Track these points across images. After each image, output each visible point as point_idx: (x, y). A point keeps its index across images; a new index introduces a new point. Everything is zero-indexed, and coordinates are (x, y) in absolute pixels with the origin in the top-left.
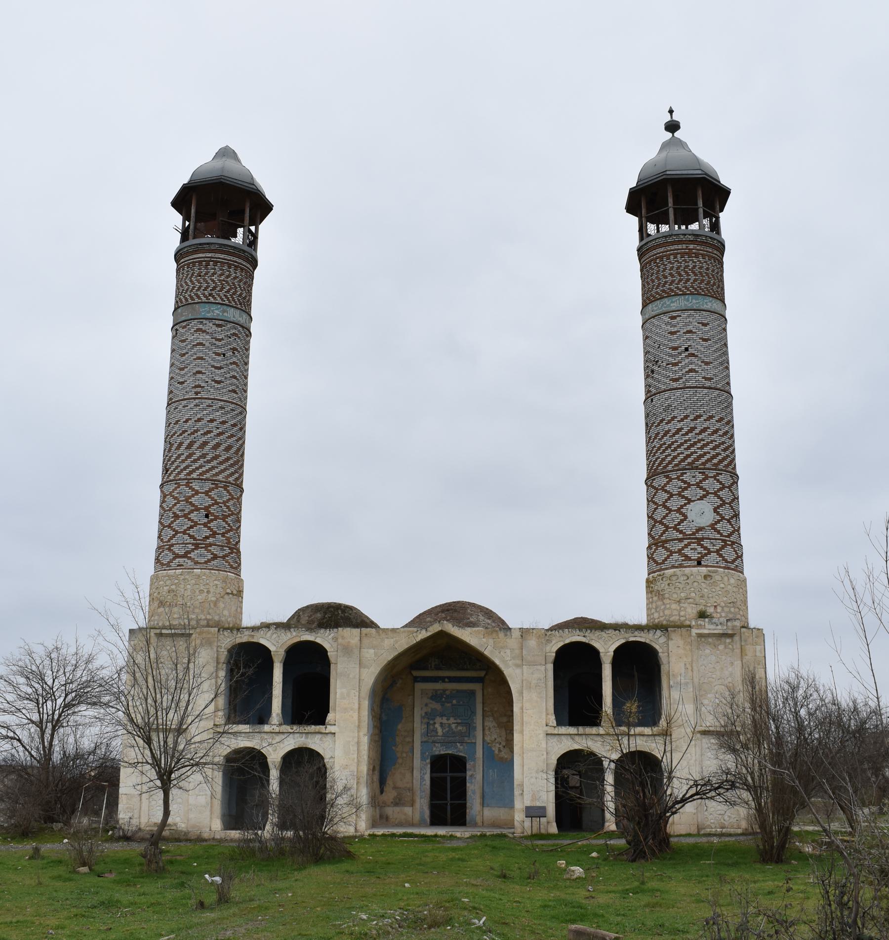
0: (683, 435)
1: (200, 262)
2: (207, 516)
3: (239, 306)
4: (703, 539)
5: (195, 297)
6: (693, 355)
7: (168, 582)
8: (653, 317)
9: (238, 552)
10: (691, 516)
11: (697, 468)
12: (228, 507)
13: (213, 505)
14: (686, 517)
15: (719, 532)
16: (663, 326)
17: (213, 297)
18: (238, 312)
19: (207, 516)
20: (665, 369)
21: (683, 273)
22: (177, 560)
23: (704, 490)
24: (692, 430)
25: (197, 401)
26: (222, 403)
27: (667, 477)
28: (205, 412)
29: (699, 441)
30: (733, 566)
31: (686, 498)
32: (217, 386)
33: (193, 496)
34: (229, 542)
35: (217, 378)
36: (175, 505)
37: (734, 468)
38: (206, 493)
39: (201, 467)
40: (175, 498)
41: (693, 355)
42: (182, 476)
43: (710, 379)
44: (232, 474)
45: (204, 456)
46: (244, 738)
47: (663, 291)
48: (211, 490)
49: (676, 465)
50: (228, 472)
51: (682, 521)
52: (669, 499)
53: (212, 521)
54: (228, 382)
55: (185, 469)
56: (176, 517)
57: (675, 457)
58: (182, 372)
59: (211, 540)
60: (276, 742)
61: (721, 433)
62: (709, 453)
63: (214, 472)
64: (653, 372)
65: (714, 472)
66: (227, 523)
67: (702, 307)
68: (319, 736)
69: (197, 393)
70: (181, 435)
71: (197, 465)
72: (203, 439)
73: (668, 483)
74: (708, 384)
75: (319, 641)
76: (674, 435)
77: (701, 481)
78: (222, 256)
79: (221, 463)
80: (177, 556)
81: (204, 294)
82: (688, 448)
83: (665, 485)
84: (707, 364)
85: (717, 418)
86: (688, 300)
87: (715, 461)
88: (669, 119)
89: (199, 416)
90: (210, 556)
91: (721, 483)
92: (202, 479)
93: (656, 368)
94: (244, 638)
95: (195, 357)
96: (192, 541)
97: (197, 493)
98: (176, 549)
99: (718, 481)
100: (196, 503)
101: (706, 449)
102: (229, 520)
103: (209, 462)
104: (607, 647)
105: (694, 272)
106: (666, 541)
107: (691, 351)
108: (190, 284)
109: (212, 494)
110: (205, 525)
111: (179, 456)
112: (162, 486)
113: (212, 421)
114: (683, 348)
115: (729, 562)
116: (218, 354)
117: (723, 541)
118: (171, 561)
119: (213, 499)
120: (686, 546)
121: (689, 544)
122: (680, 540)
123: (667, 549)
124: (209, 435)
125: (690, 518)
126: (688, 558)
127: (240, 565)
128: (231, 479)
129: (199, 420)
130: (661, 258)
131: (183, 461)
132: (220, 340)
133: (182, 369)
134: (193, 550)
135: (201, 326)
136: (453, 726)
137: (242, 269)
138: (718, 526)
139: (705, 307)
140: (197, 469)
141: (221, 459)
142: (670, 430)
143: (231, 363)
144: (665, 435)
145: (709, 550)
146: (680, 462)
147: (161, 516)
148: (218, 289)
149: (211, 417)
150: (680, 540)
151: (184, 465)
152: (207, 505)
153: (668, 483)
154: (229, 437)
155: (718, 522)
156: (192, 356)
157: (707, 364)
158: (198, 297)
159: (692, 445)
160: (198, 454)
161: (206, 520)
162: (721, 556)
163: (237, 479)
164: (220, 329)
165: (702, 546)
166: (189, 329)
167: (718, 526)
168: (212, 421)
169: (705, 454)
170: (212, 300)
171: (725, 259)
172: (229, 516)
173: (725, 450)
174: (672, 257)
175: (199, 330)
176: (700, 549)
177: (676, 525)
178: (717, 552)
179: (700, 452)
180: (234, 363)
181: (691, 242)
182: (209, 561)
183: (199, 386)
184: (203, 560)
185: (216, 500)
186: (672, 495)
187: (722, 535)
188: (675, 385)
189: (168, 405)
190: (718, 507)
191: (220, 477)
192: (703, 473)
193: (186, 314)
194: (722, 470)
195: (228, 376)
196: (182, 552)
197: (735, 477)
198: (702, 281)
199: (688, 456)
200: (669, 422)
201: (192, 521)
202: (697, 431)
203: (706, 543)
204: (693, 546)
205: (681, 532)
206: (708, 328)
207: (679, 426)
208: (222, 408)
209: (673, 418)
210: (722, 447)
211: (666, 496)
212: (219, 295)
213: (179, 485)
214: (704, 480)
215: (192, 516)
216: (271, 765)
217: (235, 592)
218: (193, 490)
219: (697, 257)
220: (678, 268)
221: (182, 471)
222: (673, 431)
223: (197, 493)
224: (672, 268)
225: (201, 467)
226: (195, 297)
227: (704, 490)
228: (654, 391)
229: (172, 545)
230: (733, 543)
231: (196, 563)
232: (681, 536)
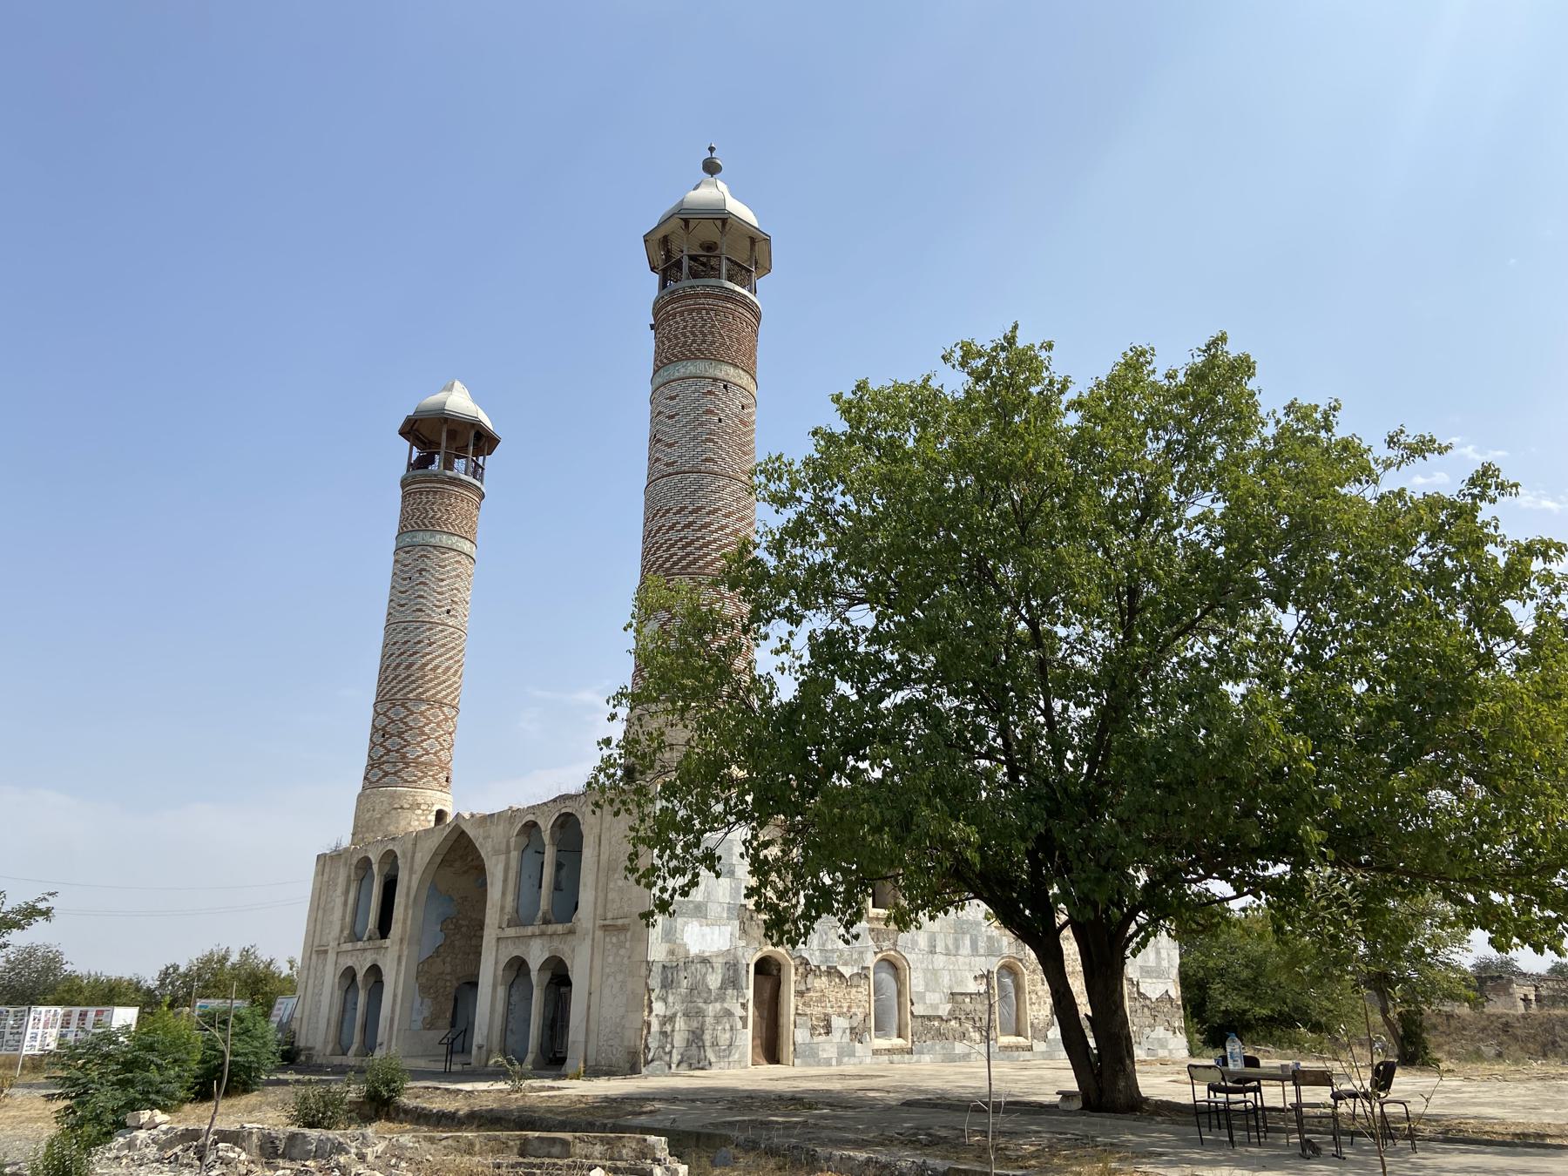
6: (659, 441)
34: (404, 756)
38: (385, 714)
41: (659, 441)
84: (670, 446)
87: (668, 565)
102: (406, 736)
104: (546, 825)
157: (670, 446)
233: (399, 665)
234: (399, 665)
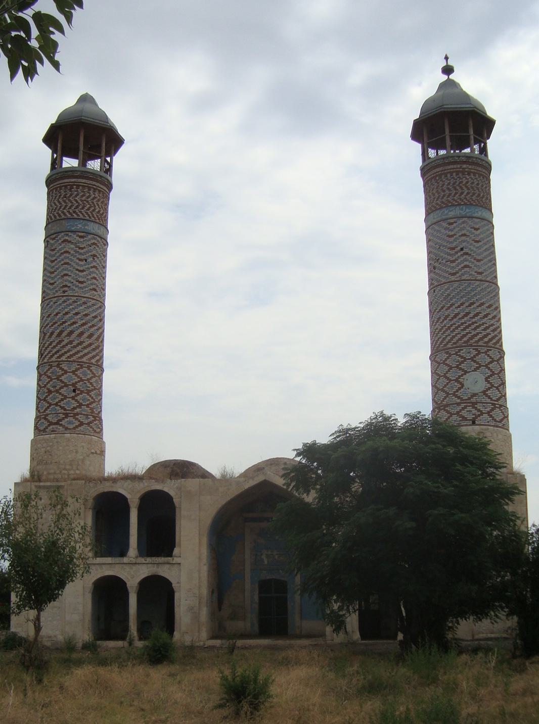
0: (459, 319)
1: (66, 186)
2: (74, 391)
3: (98, 221)
4: (476, 403)
5: (62, 214)
6: (467, 254)
7: (45, 445)
8: (435, 224)
9: (101, 420)
10: (467, 384)
11: (471, 345)
12: (91, 383)
13: (79, 382)
14: (463, 385)
15: (489, 397)
16: (443, 231)
17: (77, 214)
18: (97, 225)
19: (74, 391)
20: (445, 265)
21: (458, 188)
22: (51, 427)
23: (477, 363)
24: (467, 314)
25: (65, 298)
26: (85, 299)
27: (447, 353)
28: (71, 307)
29: (473, 323)
30: (500, 425)
31: (463, 370)
32: (80, 285)
33: (63, 375)
34: (93, 412)
35: (81, 279)
36: (48, 382)
37: (501, 345)
38: (73, 372)
39: (69, 351)
40: (49, 377)
41: (467, 254)
42: (54, 359)
43: (480, 273)
44: (94, 357)
45: (71, 342)
46: (106, 567)
47: (443, 202)
48: (77, 370)
49: (455, 343)
50: (90, 355)
51: (460, 389)
52: (449, 371)
53: (78, 394)
54: (89, 282)
55: (56, 353)
56: (50, 392)
57: (454, 337)
58: (53, 275)
59: (78, 410)
60: (133, 570)
61: (490, 317)
62: (481, 333)
63: (79, 355)
64: (435, 268)
65: (486, 349)
66: (90, 396)
67: (474, 215)
68: (168, 566)
69: (64, 292)
70: (52, 325)
71: (65, 350)
72: (70, 329)
73: (448, 358)
74: (479, 277)
75: (166, 490)
76: (452, 319)
77: (475, 356)
78: (84, 181)
79: (85, 348)
80: (51, 424)
81: (69, 212)
82: (464, 329)
83: (446, 360)
84: (479, 261)
85: (487, 305)
86: (462, 209)
87: (486, 340)
88: (445, 64)
89: (66, 310)
90: (77, 423)
91: (490, 357)
92: (70, 361)
93: (437, 265)
94: (107, 488)
95: (62, 262)
96: (63, 411)
97: (66, 372)
98: (50, 418)
99: (488, 356)
100: (66, 381)
101: (478, 330)
102: (92, 394)
103: (75, 347)
105: (466, 187)
106: (447, 405)
107: (465, 250)
108: (57, 203)
109: (78, 373)
110: (73, 398)
111: (50, 344)
112: (38, 368)
113: (77, 314)
114: (459, 248)
115: (498, 422)
116: (80, 260)
117: (493, 404)
118: (47, 428)
119: (78, 377)
120: (463, 409)
121: (465, 407)
122: (458, 404)
123: (448, 412)
124: (75, 326)
125: (466, 386)
126: (464, 419)
127: (102, 430)
128: (93, 361)
129: (67, 313)
130: (440, 176)
131: (54, 347)
132: (82, 248)
133: (53, 273)
134: (63, 419)
135: (67, 238)
136: (276, 557)
137: (100, 191)
138: (489, 392)
139: (476, 215)
140: (66, 353)
141: (84, 345)
142: (449, 315)
143: (92, 267)
144: (445, 319)
145: (481, 411)
146: (458, 341)
147: (38, 391)
148: (80, 207)
149: (76, 311)
150: (458, 404)
151: (55, 350)
152: (74, 381)
153: (448, 358)
154: (91, 327)
155: (489, 389)
156: (60, 262)
157: (479, 261)
158: (65, 214)
159: (467, 327)
160: (66, 341)
161: (73, 394)
162: (491, 416)
163: (98, 361)
164: (82, 240)
165: (476, 408)
166: (58, 241)
167: (489, 392)
168: (77, 314)
169: (478, 334)
170: (75, 216)
171: (491, 177)
172: (92, 390)
173: (494, 331)
174: (449, 175)
175: (65, 241)
176: (474, 411)
177: (455, 392)
178: (488, 413)
179: (473, 333)
180: (94, 267)
181: (464, 163)
182: (77, 427)
183: (66, 286)
184: (71, 427)
185: (81, 378)
186: (451, 368)
187: (491, 399)
188: (453, 278)
189: (42, 302)
190: (489, 377)
191: (84, 359)
192: (476, 350)
193: (56, 228)
194: (491, 347)
195: (89, 277)
196: (55, 420)
197: (502, 353)
198: (474, 194)
199: (464, 336)
200: (449, 308)
201: (63, 395)
202: (471, 315)
203: (479, 406)
204: (469, 408)
205: (459, 397)
206: (478, 232)
207: (456, 311)
208: (85, 303)
209: (451, 306)
210: (491, 328)
211: (447, 368)
212: (81, 212)
213: (51, 366)
214: (477, 355)
215: (62, 391)
216: (130, 590)
217: (98, 452)
218: (63, 370)
219: (469, 174)
220: (454, 183)
221: (53, 355)
222: (452, 315)
223: (66, 372)
224: (449, 184)
225: (69, 351)
226: (62, 214)
227: (477, 363)
228: (436, 284)
229: (47, 415)
230: (501, 406)
231: (67, 429)
232: (459, 401)
233: (82, 333)
234: (82, 333)
